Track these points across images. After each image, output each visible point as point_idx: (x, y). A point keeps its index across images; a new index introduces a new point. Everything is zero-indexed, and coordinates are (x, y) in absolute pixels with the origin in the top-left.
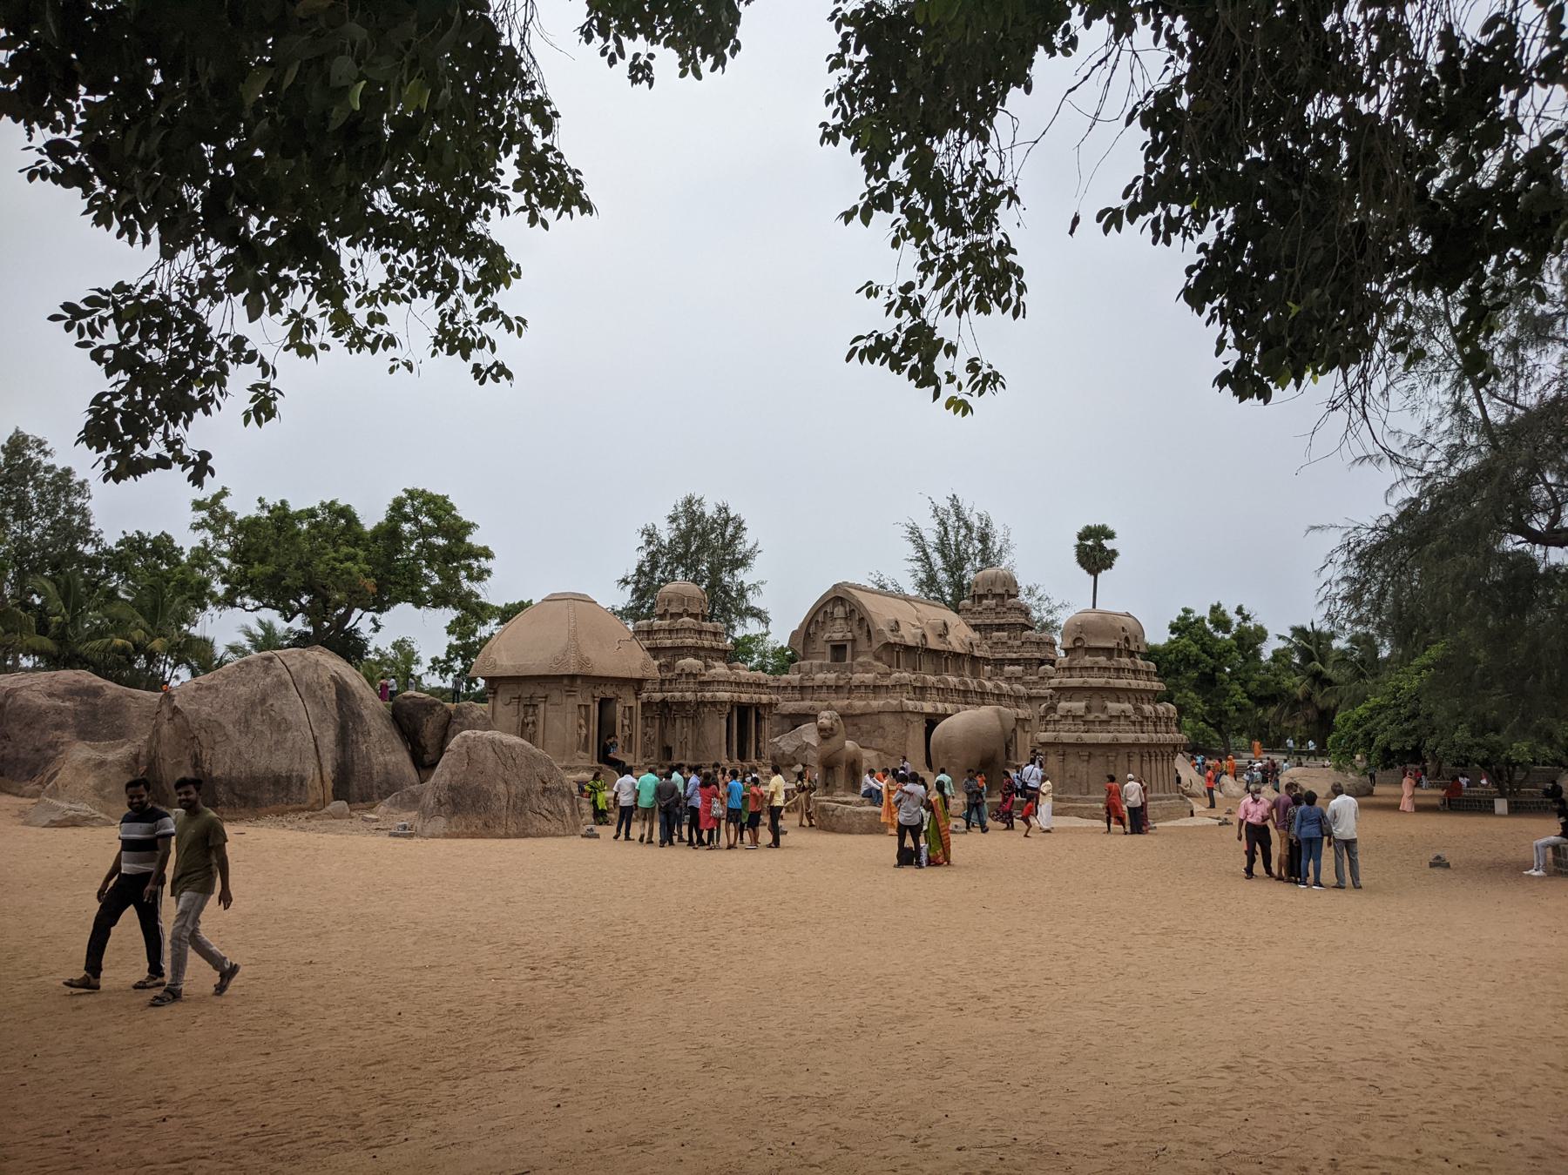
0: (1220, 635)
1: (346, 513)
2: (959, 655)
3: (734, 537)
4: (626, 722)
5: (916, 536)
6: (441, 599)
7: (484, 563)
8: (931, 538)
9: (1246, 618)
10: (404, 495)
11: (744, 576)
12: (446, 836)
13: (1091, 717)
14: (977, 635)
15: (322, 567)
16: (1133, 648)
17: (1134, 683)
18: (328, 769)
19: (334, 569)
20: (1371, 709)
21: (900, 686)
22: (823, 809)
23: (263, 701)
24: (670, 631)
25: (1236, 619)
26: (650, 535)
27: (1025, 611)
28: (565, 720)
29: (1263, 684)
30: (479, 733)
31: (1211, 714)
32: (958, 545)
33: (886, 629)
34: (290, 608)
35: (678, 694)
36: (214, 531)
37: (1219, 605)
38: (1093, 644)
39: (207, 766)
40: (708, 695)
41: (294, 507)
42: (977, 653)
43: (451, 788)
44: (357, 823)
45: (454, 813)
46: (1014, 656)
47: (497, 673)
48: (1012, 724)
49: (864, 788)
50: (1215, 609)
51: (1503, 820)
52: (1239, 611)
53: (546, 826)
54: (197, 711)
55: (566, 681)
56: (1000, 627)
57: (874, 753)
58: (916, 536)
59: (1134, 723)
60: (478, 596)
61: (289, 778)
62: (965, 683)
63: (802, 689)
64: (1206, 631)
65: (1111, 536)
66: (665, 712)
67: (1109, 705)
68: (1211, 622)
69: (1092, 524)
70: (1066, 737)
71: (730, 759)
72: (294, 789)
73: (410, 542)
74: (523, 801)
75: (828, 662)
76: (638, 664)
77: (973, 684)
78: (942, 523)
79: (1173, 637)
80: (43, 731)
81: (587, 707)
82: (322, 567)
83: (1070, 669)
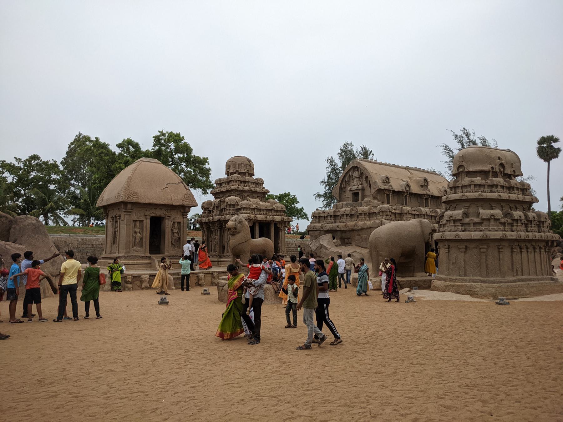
5: (448, 150)
10: (159, 134)
13: (467, 220)
16: (509, 171)
17: (505, 195)
21: (383, 212)
26: (331, 162)
38: (471, 168)
48: (428, 231)
57: (368, 250)
59: (504, 224)
65: (556, 140)
69: (545, 136)
75: (350, 202)
78: (461, 142)
81: (141, 222)
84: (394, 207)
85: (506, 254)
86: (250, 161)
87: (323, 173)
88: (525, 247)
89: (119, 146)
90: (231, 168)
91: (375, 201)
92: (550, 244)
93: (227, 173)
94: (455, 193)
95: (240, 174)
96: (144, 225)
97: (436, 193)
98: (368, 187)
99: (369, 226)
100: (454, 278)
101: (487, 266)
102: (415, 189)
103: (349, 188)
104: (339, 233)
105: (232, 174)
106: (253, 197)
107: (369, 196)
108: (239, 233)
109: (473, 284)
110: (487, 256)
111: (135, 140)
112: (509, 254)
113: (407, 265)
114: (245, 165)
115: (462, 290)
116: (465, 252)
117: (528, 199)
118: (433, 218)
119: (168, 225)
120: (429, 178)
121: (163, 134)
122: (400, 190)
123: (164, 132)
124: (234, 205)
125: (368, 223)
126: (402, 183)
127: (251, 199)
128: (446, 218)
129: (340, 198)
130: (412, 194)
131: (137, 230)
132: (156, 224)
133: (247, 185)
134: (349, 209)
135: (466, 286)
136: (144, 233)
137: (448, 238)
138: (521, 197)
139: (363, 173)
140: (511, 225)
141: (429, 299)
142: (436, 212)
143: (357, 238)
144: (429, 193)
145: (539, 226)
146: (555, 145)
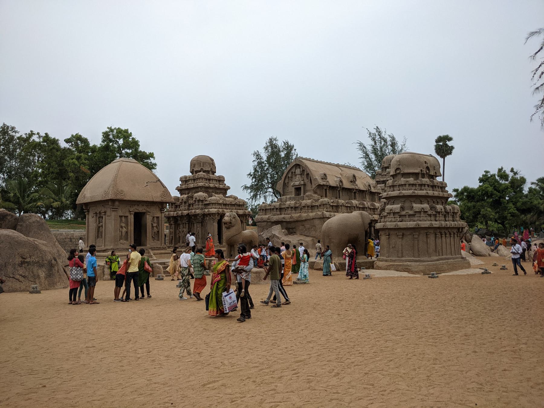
0: (503, 182)
2: (363, 191)
5: (362, 146)
7: (152, 160)
8: (369, 148)
9: (516, 173)
13: (403, 213)
17: (431, 193)
21: (323, 205)
25: (511, 174)
29: (524, 203)
31: (499, 218)
32: (381, 148)
37: (502, 168)
40: (206, 210)
42: (373, 190)
50: (500, 170)
52: (512, 170)
53: (17, 285)
57: (311, 239)
58: (362, 146)
59: (430, 215)
64: (496, 181)
68: (498, 176)
75: (293, 196)
78: (374, 139)
79: (481, 184)
81: (126, 217)
84: (332, 201)
85: (432, 237)
86: (212, 160)
87: (250, 166)
88: (444, 233)
89: (67, 141)
90: (196, 166)
91: (316, 195)
92: (461, 230)
93: (192, 172)
94: (394, 191)
95: (204, 172)
96: (129, 220)
97: (362, 188)
98: (309, 183)
99: (312, 218)
100: (394, 259)
101: (418, 249)
103: (292, 184)
104: (285, 224)
105: (197, 172)
106: (217, 193)
107: (309, 191)
108: (233, 226)
109: (409, 263)
110: (418, 240)
111: (84, 136)
112: (434, 239)
113: (356, 250)
114: (209, 164)
115: (400, 268)
117: (446, 195)
118: (348, 208)
119: (149, 219)
120: (357, 174)
121: (111, 130)
122: (335, 185)
123: (113, 128)
124: (202, 201)
126: (336, 179)
127: (216, 195)
128: (387, 211)
129: (283, 192)
131: (123, 225)
132: (139, 218)
133: (211, 182)
134: (293, 202)
135: (403, 265)
136: (129, 228)
137: (389, 227)
138: (441, 194)
139: (304, 170)
140: (435, 216)
141: (378, 276)
142: (363, 204)
143: (301, 227)
144: (357, 188)
145: (453, 217)
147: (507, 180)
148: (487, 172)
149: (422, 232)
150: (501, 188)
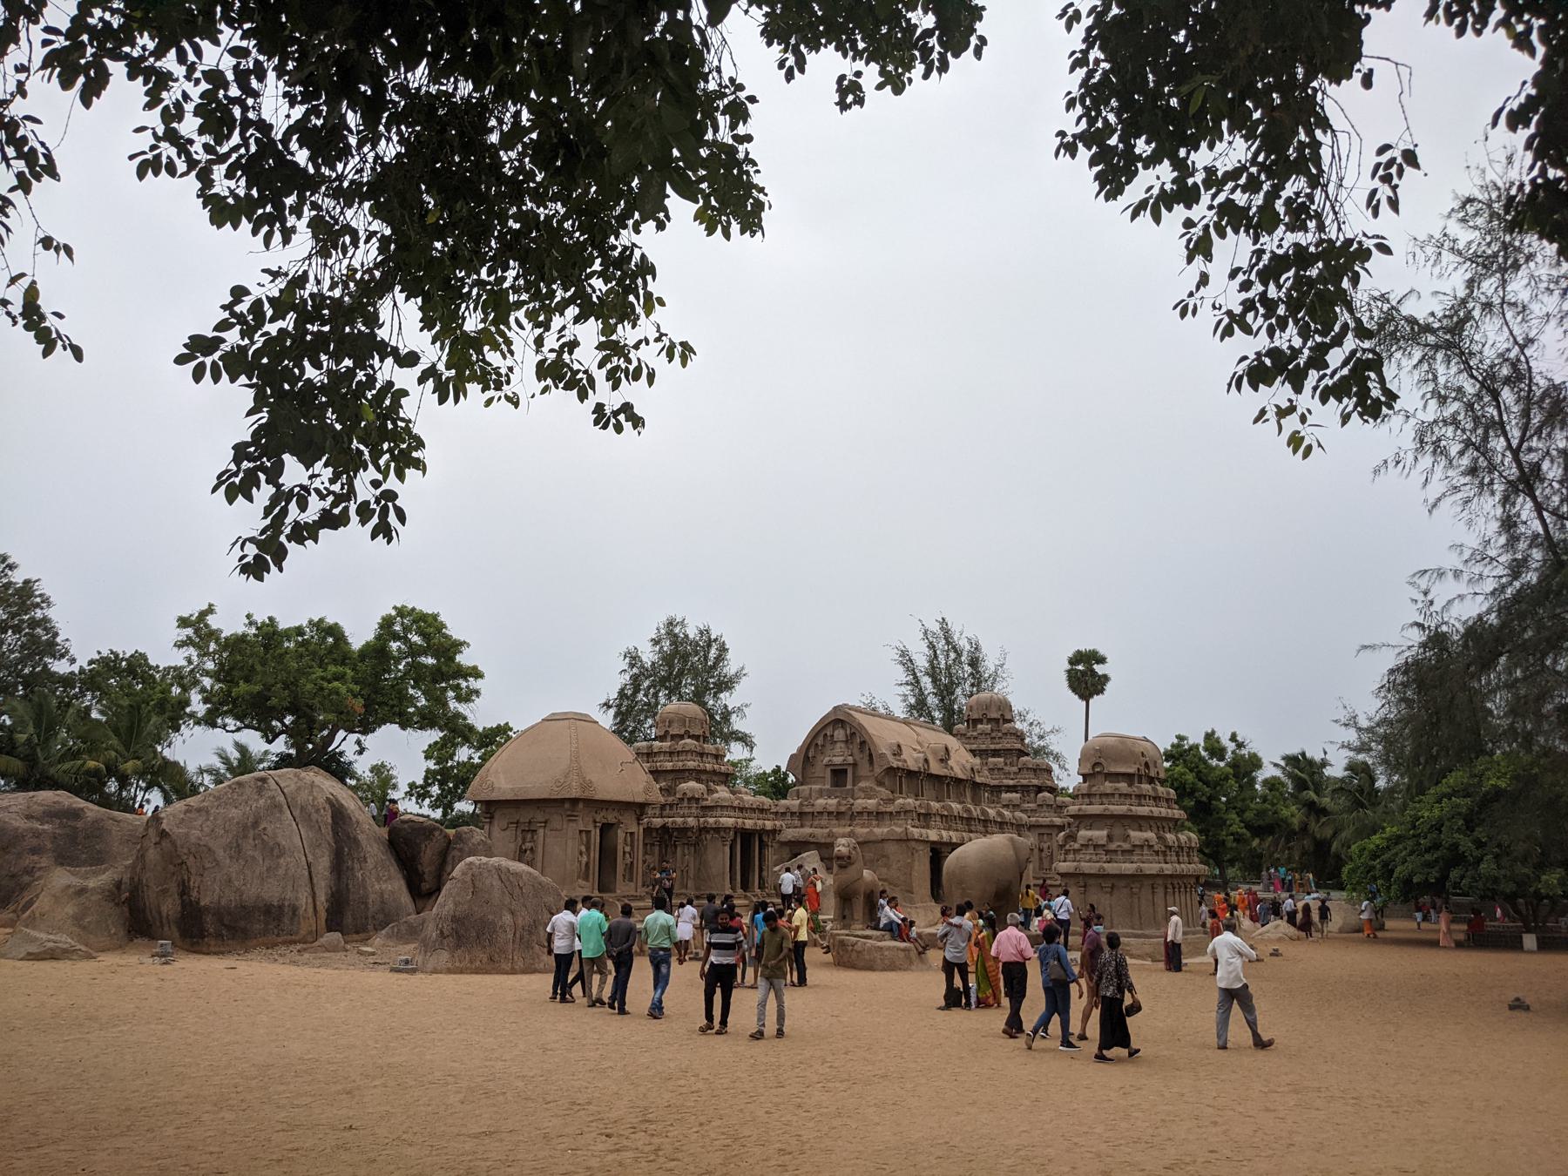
0: (1214, 762)
1: (335, 631)
3: (720, 658)
4: (628, 849)
5: (906, 660)
6: (426, 721)
7: (473, 683)
8: (922, 662)
9: (1240, 745)
10: (394, 613)
11: (729, 699)
12: (449, 971)
13: (1113, 846)
14: (977, 761)
15: (309, 686)
16: (1152, 774)
17: (1156, 811)
18: (322, 898)
19: (322, 689)
20: (1388, 839)
21: (905, 812)
22: (842, 943)
23: (256, 824)
24: (671, 753)
25: (1231, 746)
26: (633, 658)
27: (1020, 736)
28: (566, 846)
29: (1260, 814)
30: (484, 859)
31: (1207, 844)
32: (948, 668)
33: (888, 754)
34: (272, 729)
35: (679, 820)
36: (194, 645)
37: (1213, 732)
38: (1113, 770)
39: (194, 894)
40: (711, 820)
41: (283, 625)
42: (978, 780)
43: (455, 919)
44: (352, 957)
45: (458, 946)
46: (1011, 783)
47: (494, 796)
49: (883, 921)
50: (1209, 736)
51: (1535, 957)
52: (1233, 738)
54: (187, 834)
55: (567, 805)
56: (996, 753)
58: (906, 660)
59: (1157, 853)
60: (465, 718)
61: (281, 907)
62: (968, 811)
63: (802, 815)
64: (1201, 759)
65: (1102, 660)
66: (665, 838)
67: (1132, 833)
68: (1206, 749)
70: (1087, 868)
71: (733, 888)
72: (286, 920)
73: (398, 661)
74: (530, 933)
75: (828, 786)
76: (641, 787)
77: (976, 812)
78: (932, 646)
80: (20, 856)
82: (309, 686)
83: (1089, 795)
102: (935, 768)
107: (866, 778)
116: (1111, 893)
125: (877, 831)
130: (931, 776)
140: (1164, 854)
146: (1099, 669)
147: (1222, 758)
148: (1181, 738)
149: (1147, 882)
150: (1212, 777)
